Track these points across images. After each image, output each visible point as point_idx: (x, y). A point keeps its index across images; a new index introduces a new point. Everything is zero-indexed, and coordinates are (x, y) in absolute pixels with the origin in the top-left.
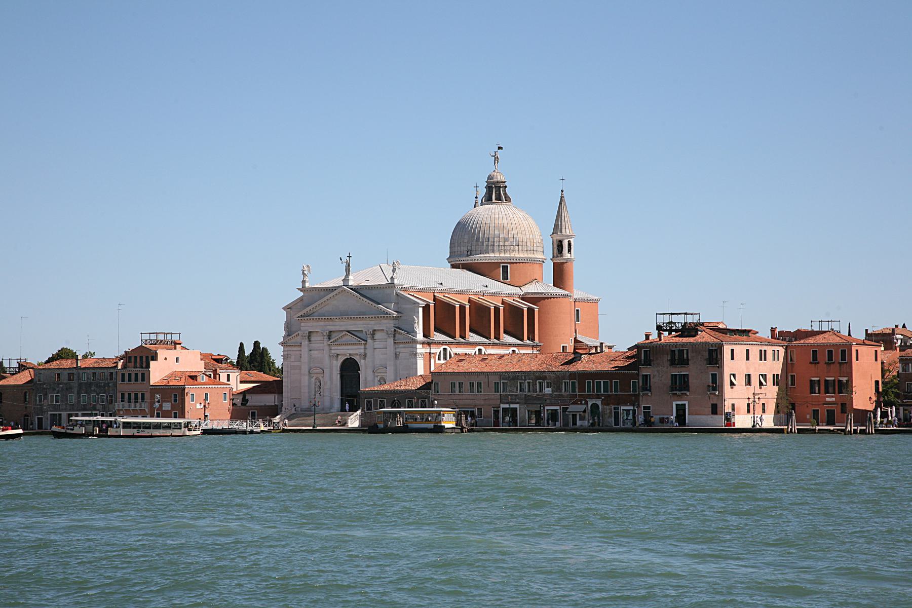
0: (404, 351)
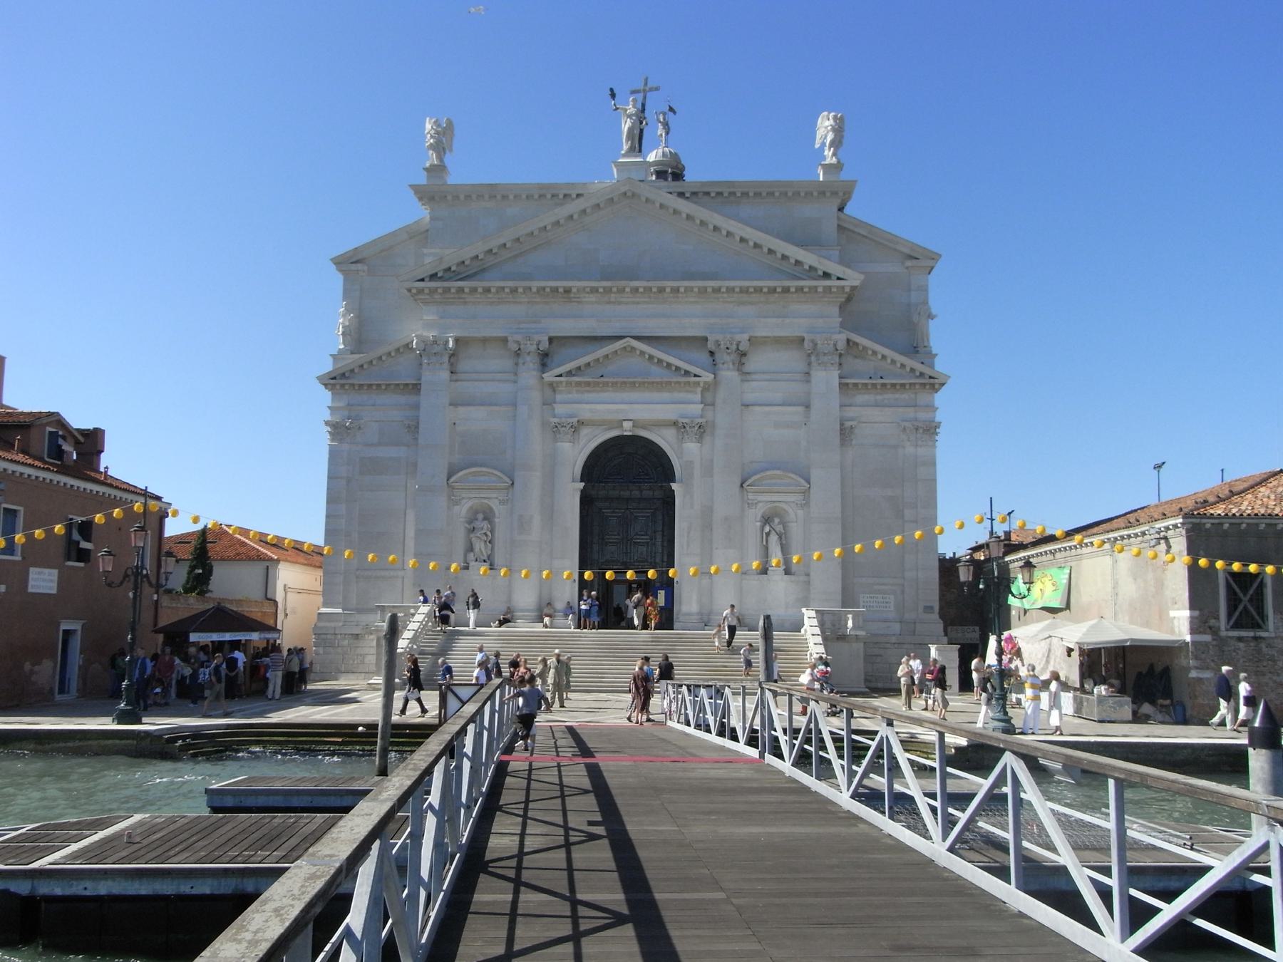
0: (877, 419)
